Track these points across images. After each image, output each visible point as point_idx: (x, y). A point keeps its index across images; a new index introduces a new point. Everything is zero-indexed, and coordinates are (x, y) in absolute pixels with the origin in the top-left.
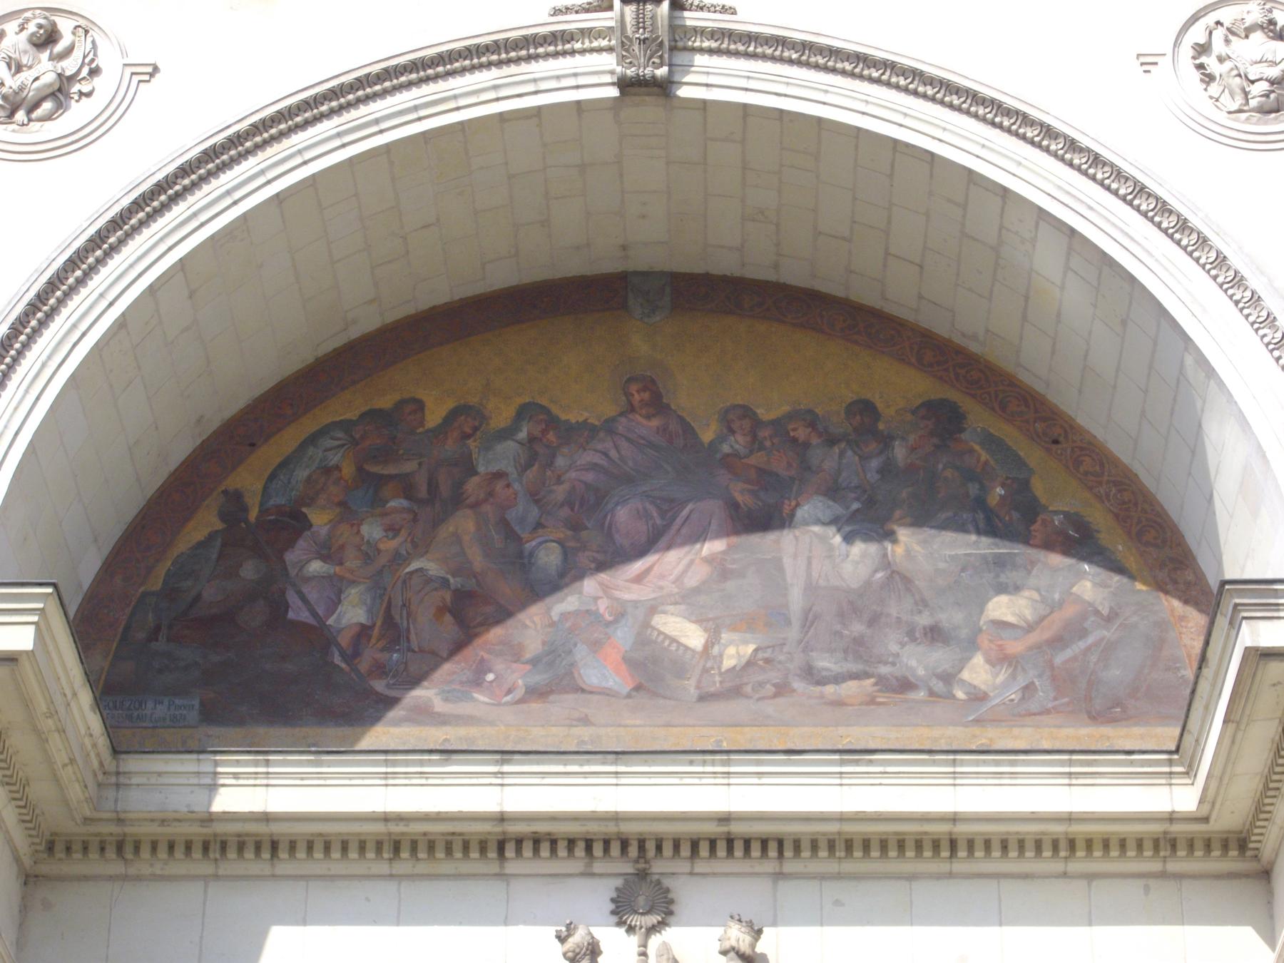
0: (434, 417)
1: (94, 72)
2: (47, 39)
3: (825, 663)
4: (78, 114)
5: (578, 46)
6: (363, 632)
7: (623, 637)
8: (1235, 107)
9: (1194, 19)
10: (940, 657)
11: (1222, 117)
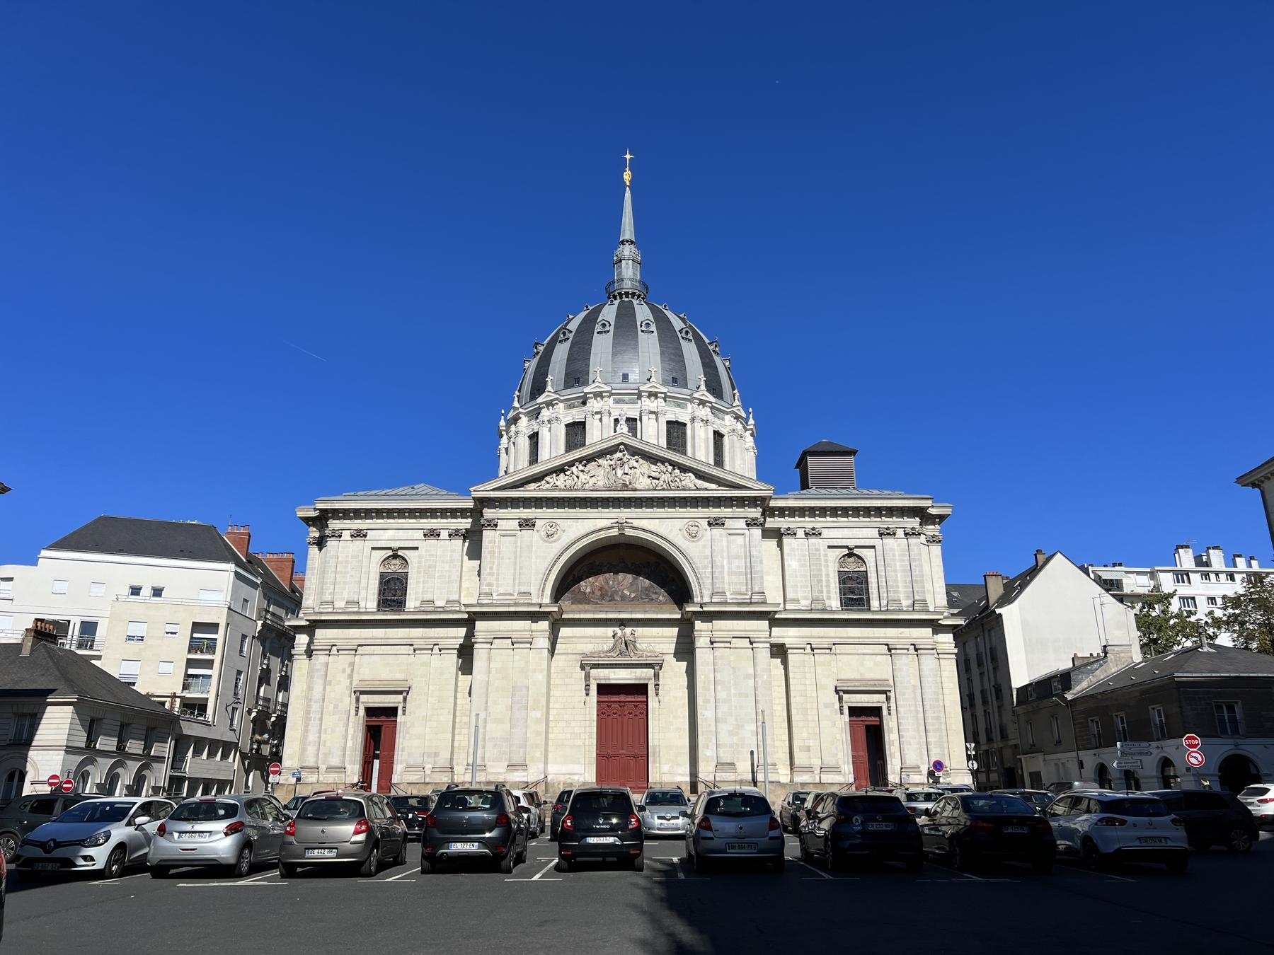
0: (597, 563)
3: (643, 597)
4: (556, 536)
6: (590, 593)
7: (620, 593)
10: (656, 596)
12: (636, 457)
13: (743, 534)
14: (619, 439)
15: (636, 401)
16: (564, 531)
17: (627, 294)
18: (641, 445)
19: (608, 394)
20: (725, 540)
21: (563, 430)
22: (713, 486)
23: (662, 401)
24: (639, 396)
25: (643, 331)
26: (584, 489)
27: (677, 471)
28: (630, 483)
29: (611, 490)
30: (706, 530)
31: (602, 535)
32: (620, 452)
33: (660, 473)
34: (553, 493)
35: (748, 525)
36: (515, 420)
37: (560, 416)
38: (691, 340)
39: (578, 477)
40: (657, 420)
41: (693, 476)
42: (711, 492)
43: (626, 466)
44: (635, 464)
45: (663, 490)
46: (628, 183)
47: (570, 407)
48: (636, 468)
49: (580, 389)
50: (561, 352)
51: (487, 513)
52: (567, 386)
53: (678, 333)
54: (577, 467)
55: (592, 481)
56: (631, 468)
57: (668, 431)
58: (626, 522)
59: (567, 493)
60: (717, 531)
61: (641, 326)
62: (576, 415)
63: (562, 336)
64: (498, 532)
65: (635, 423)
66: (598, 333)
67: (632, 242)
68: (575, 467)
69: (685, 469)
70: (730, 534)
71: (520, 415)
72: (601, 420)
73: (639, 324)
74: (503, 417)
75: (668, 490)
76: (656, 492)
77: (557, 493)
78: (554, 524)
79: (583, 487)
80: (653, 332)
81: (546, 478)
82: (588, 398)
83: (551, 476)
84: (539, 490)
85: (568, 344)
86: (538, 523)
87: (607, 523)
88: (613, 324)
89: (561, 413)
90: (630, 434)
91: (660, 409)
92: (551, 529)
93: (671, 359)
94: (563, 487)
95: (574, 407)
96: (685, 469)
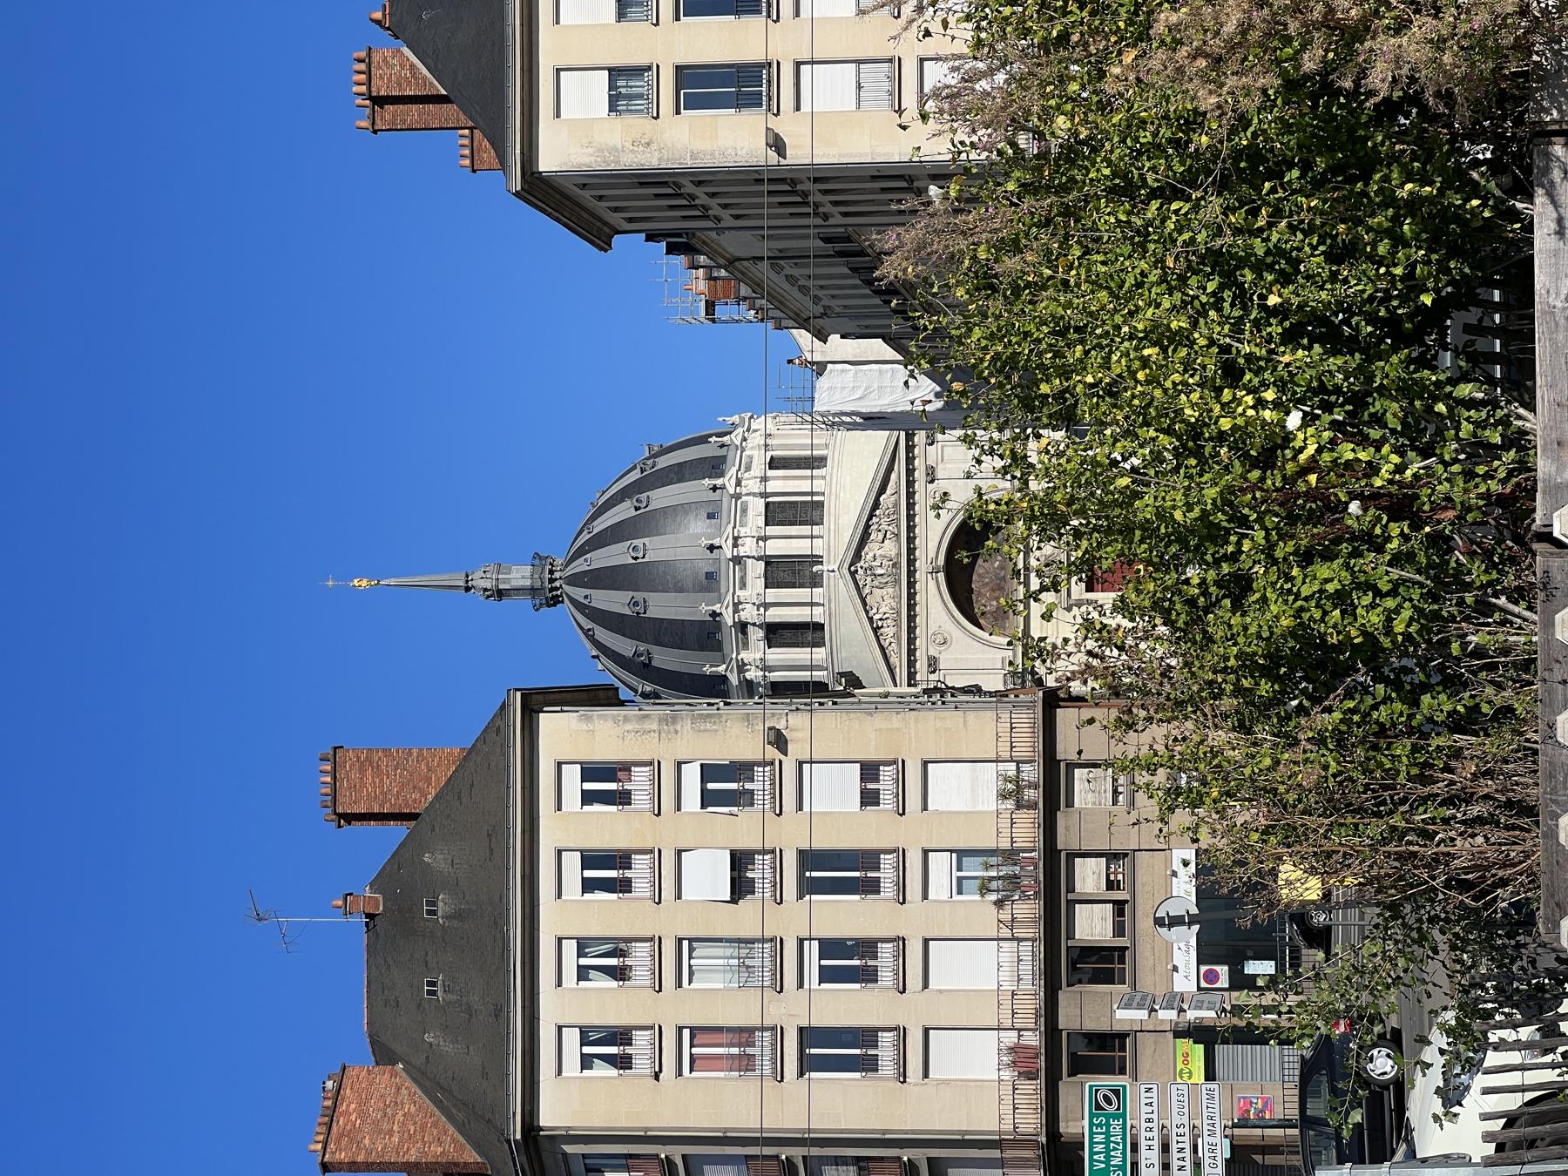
20: (948, 466)
22: (893, 476)
27: (878, 512)
35: (931, 444)
41: (883, 496)
44: (871, 555)
47: (746, 645)
50: (664, 658)
52: (718, 647)
55: (888, 601)
60: (940, 474)
62: (756, 635)
85: (654, 649)
87: (932, 584)
88: (631, 594)
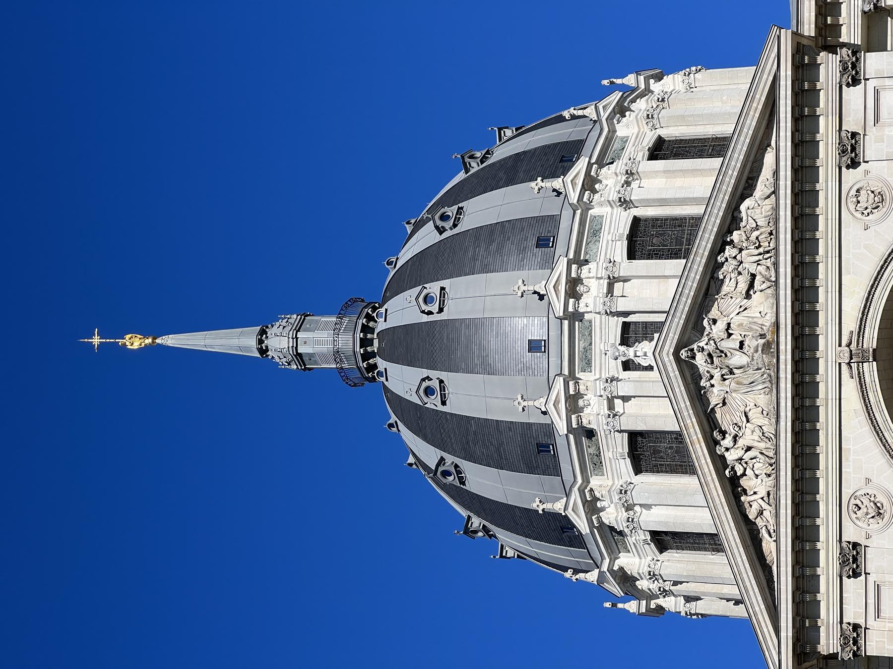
1: (868, 494)
2: (857, 505)
4: (881, 498)
5: (862, 371)
8: (881, 206)
9: (852, 214)
11: (885, 209)
12: (705, 323)
13: (877, 92)
14: (666, 359)
15: (587, 324)
16: (868, 480)
17: (365, 343)
18: (678, 314)
19: (571, 383)
21: (648, 480)
22: (769, 158)
23: (585, 269)
24: (575, 317)
25: (441, 310)
26: (776, 436)
27: (736, 236)
28: (762, 336)
29: (778, 378)
30: (867, 172)
31: (876, 396)
32: (694, 358)
33: (740, 273)
34: (783, 502)
35: (855, 82)
36: (626, 579)
37: (618, 483)
38: (459, 208)
39: (749, 449)
40: (625, 280)
41: (747, 203)
42: (782, 163)
43: (725, 345)
44: (721, 325)
45: (776, 265)
46: (149, 341)
47: (598, 464)
48: (729, 324)
49: (561, 443)
51: (828, 645)
52: (554, 469)
53: (445, 235)
54: (727, 449)
55: (757, 418)
56: (730, 335)
57: (649, 257)
58: (849, 345)
59: (782, 473)
60: (871, 148)
61: (430, 313)
63: (451, 478)
64: (871, 622)
65: (632, 327)
66: (444, 403)
67: (263, 332)
68: (727, 454)
69: (732, 220)
70: (877, 120)
71: (616, 568)
72: (625, 399)
73: (425, 318)
74: (620, 606)
75: (777, 255)
76: (782, 281)
77: (782, 492)
78: (853, 501)
79: (769, 439)
80: (443, 289)
81: (751, 517)
82: (581, 427)
83: (747, 505)
84: (777, 531)
85: (467, 467)
86: (850, 535)
87: (850, 387)
88: (425, 372)
89: (610, 483)
90: (656, 336)
91: (603, 273)
92: (864, 510)
93: (499, 249)
94: (770, 482)
95: (598, 455)
96: (732, 220)
